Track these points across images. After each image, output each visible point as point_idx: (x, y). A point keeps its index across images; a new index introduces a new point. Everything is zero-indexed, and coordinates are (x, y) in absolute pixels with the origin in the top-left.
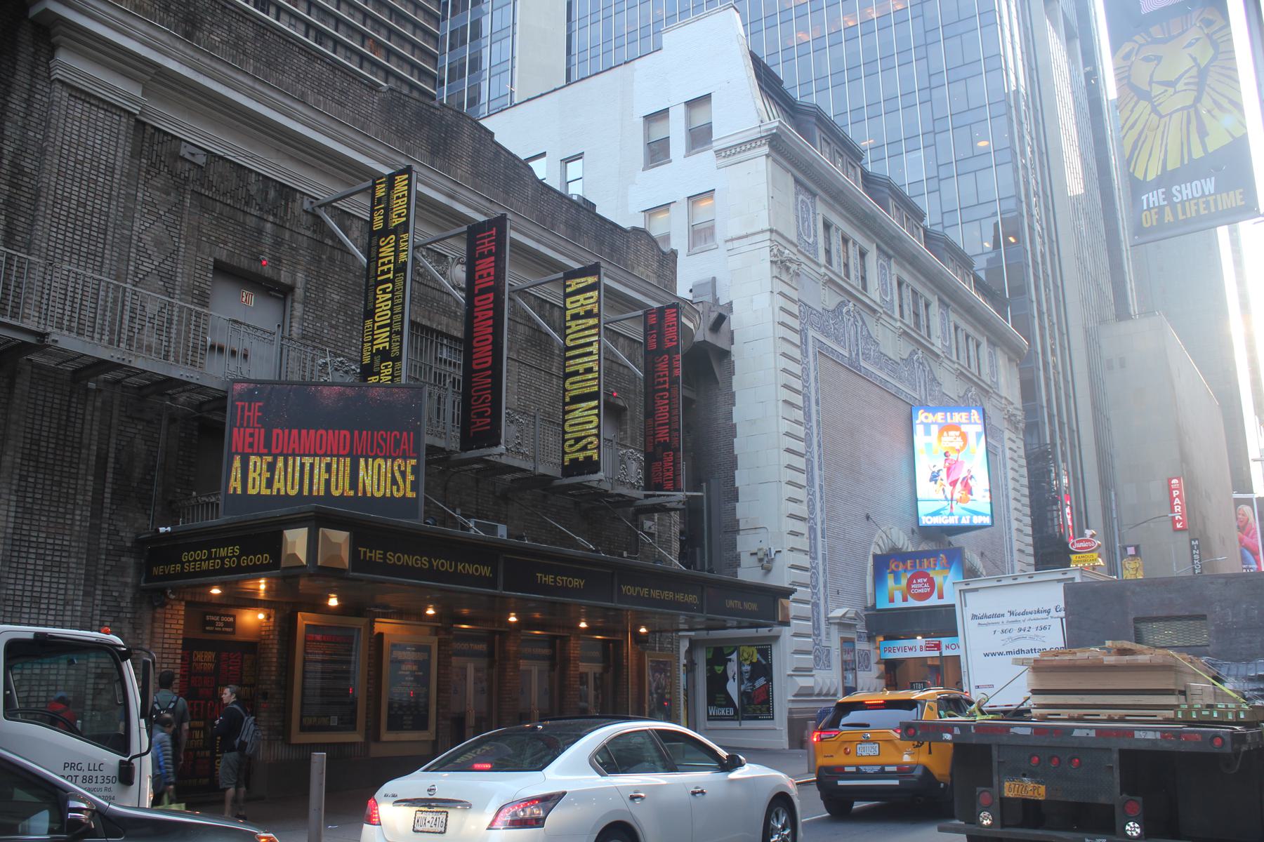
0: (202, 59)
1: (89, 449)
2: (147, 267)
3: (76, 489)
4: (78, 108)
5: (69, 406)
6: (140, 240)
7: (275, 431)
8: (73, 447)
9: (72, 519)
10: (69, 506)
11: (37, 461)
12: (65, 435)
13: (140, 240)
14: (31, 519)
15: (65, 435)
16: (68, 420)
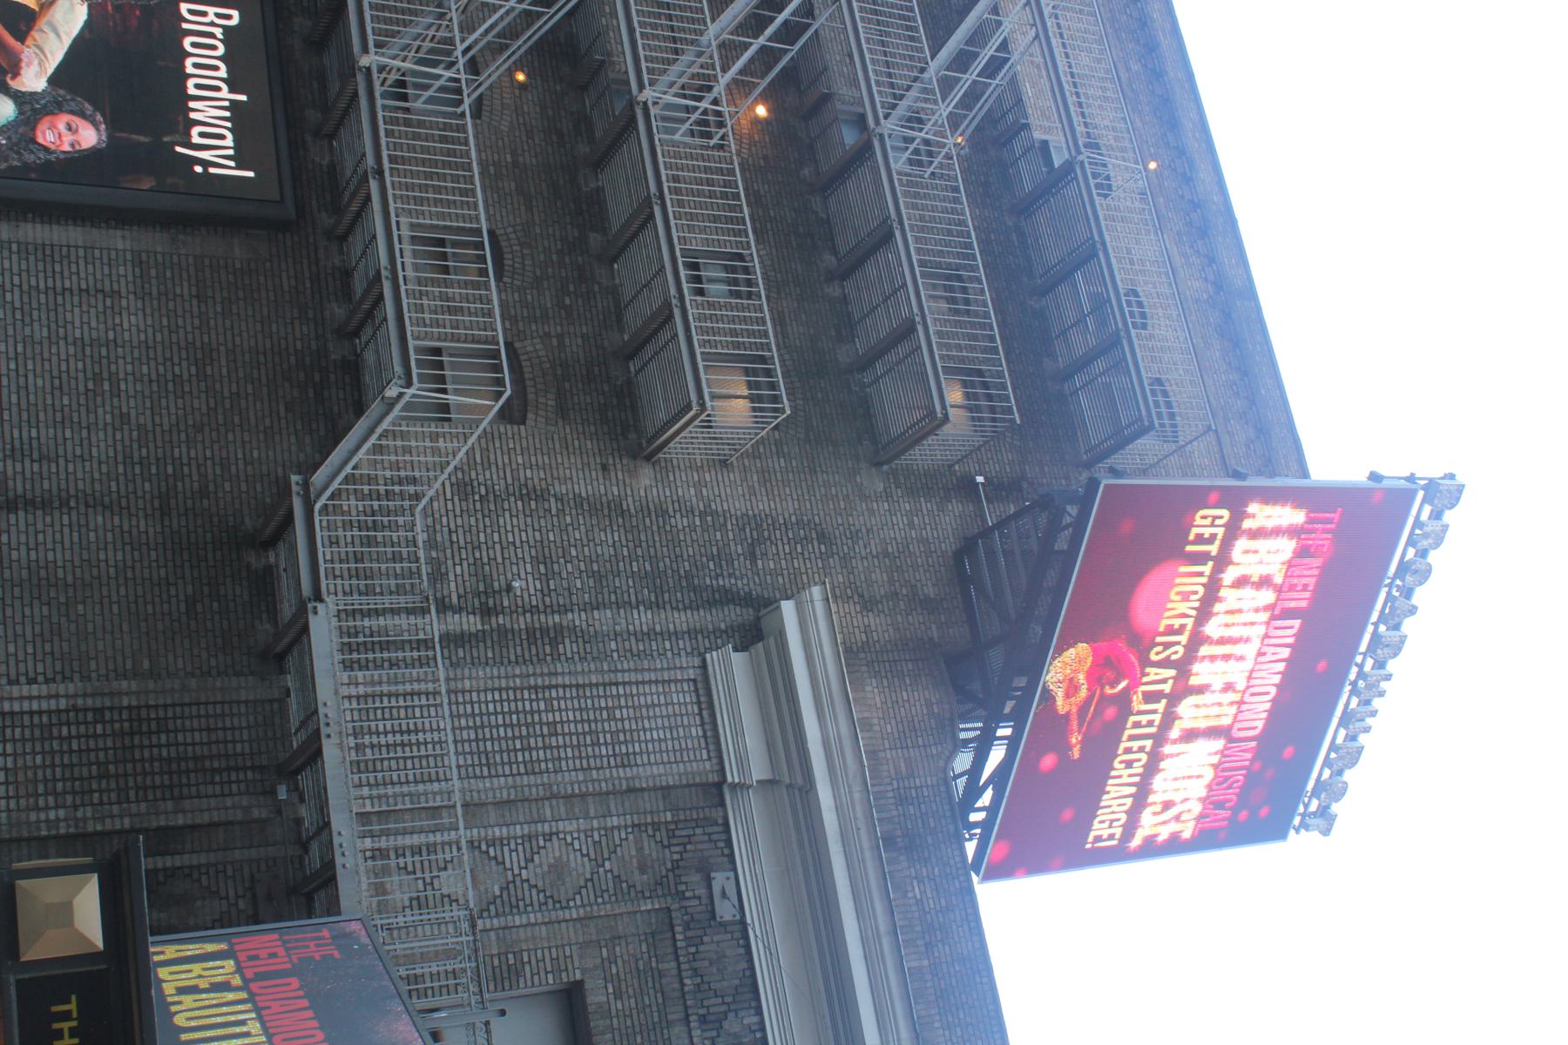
0: (863, 832)
1: (176, 812)
2: (513, 859)
3: (101, 803)
4: (683, 697)
5: (237, 769)
6: (548, 837)
7: (295, 982)
8: (171, 787)
9: (47, 808)
10: (69, 799)
11: (132, 734)
12: (188, 771)
13: (548, 837)
14: (33, 740)
15: (188, 771)
16: (214, 771)
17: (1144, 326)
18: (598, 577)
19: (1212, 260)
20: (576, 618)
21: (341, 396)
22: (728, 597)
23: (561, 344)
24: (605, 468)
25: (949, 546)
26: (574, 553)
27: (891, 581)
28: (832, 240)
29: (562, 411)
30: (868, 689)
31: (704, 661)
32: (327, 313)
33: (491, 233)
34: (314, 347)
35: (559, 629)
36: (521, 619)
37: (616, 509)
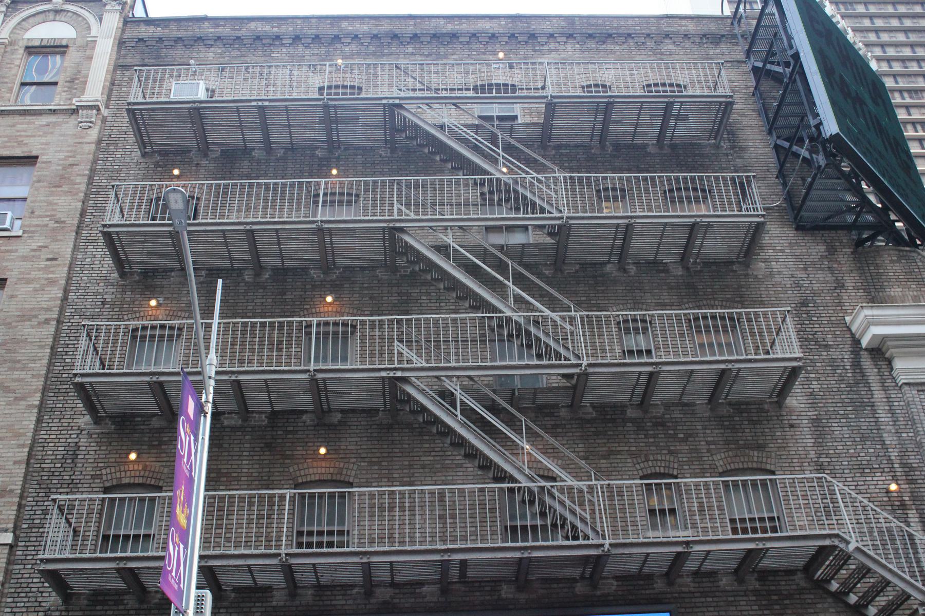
17: (360, 89)
18: (864, 439)
19: (552, 36)
20: (894, 454)
21: (783, 583)
22: (856, 364)
23: (713, 443)
24: (792, 426)
25: (791, 233)
26: (852, 451)
27: (821, 269)
28: (595, 264)
29: (760, 447)
30: (892, 294)
31: (906, 384)
32: (728, 588)
33: (641, 478)
34: (754, 598)
35: (903, 465)
36: (903, 486)
37: (816, 422)
